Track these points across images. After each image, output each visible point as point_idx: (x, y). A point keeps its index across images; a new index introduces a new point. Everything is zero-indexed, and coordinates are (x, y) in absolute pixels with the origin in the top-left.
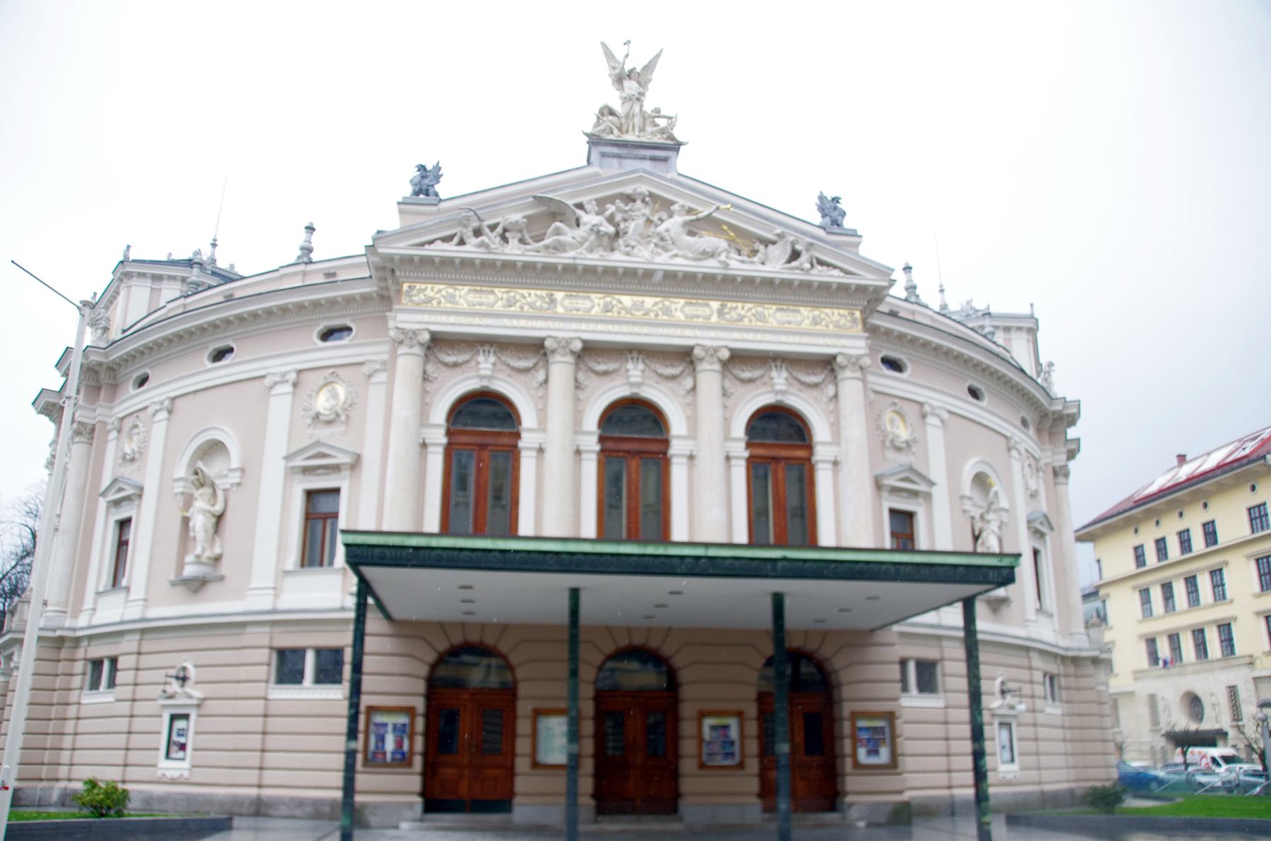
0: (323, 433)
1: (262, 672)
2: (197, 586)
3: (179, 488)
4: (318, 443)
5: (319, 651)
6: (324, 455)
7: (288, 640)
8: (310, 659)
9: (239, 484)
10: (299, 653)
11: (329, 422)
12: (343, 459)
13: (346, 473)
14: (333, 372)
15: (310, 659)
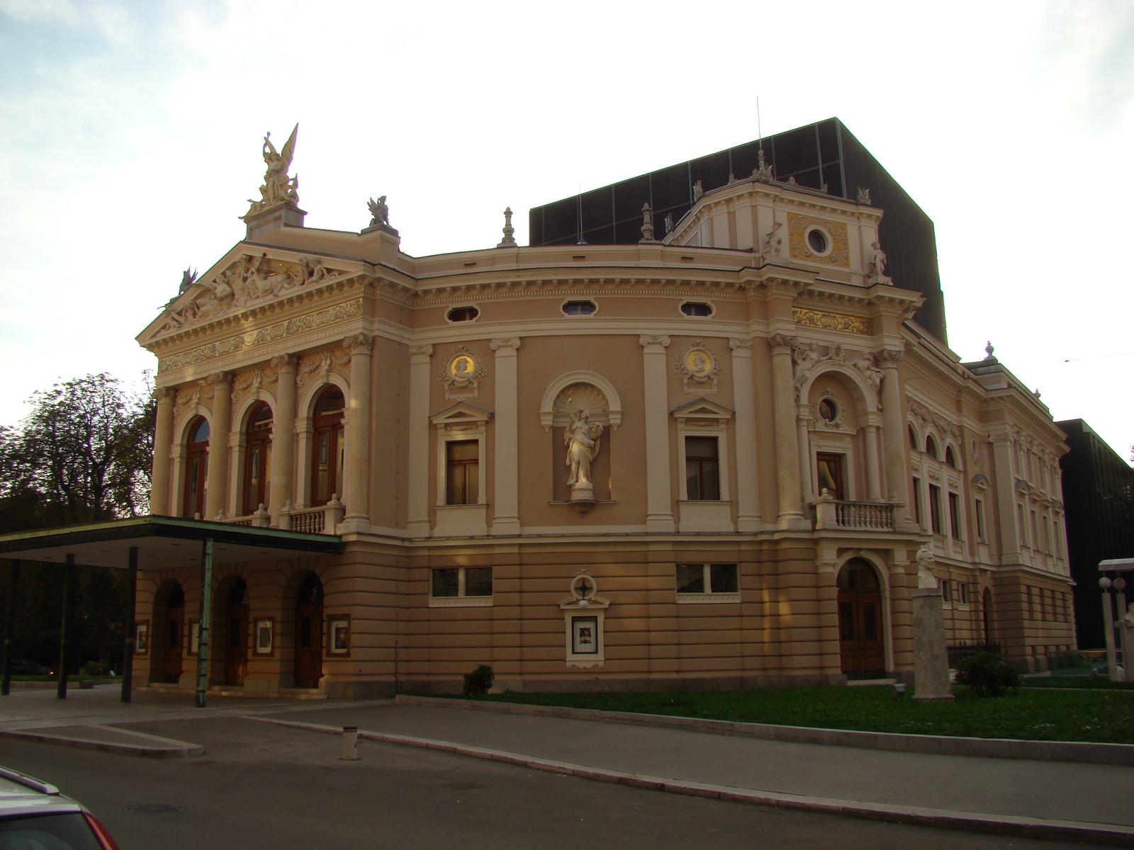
0: (701, 392)
1: (673, 582)
2: (585, 508)
3: (547, 421)
4: (703, 400)
5: (713, 566)
6: (703, 410)
7: (689, 557)
8: (707, 572)
9: (619, 426)
10: (698, 568)
11: (700, 383)
12: (723, 415)
13: (723, 426)
14: (700, 343)
15: (707, 572)
